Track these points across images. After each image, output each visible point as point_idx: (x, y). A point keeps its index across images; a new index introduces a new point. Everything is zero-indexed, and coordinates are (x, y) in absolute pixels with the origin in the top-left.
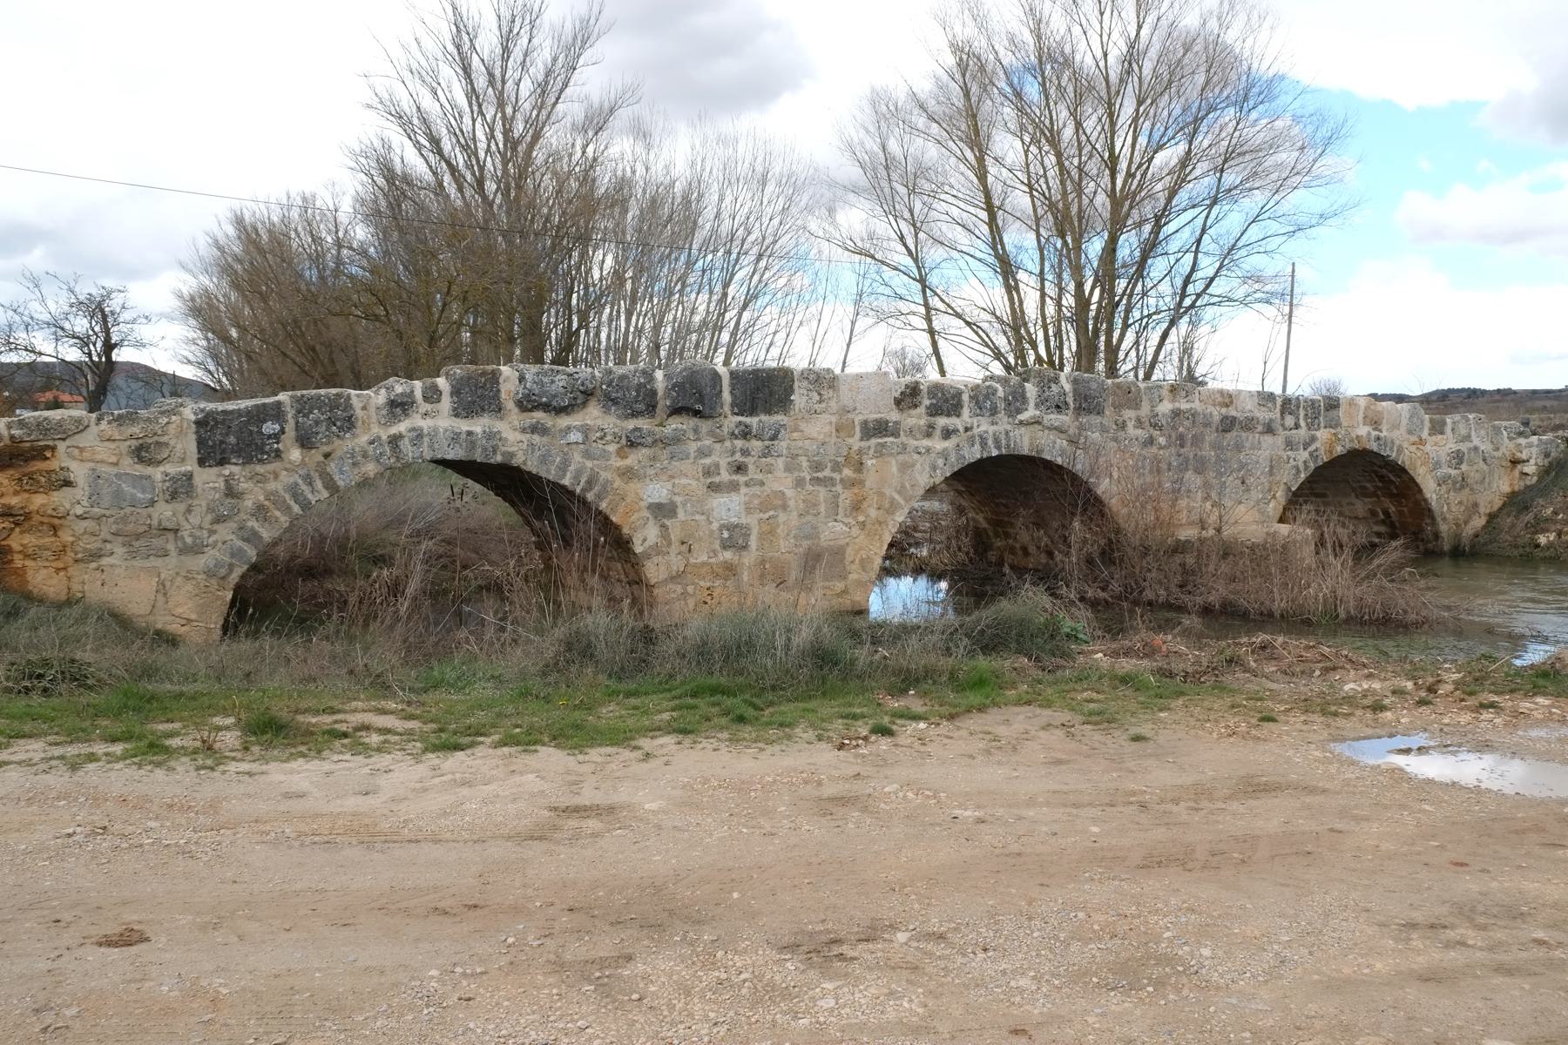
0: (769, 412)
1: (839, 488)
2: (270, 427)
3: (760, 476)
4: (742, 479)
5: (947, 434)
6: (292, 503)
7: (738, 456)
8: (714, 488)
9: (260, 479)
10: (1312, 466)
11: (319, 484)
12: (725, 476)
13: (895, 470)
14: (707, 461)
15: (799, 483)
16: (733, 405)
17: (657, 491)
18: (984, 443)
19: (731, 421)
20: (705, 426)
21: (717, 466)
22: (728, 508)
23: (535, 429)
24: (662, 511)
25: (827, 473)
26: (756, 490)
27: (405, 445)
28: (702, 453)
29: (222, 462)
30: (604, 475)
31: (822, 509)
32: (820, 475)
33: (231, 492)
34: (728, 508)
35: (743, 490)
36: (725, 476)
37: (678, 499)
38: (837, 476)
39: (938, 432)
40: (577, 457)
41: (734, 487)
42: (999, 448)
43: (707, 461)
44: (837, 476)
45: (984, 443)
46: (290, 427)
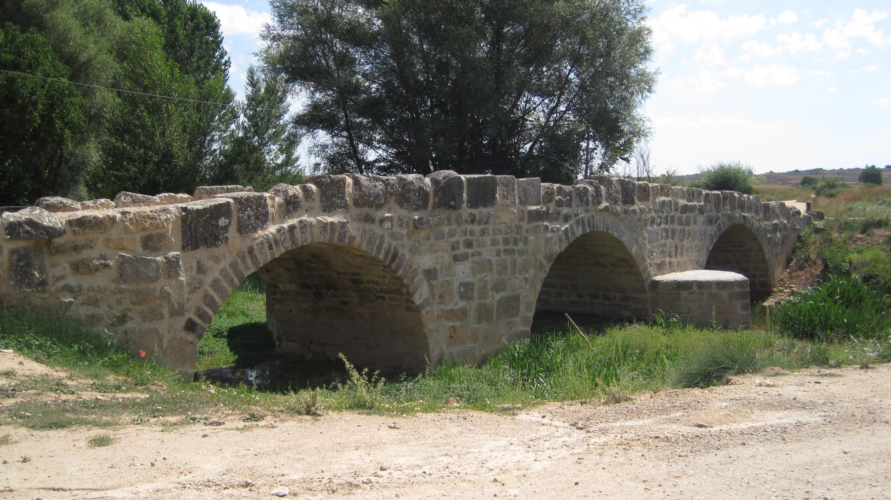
0: (485, 206)
1: (517, 256)
2: (222, 222)
3: (479, 249)
4: (470, 251)
5: (566, 219)
6: (234, 276)
7: (468, 237)
8: (456, 259)
9: (217, 260)
10: (718, 234)
11: (249, 262)
12: (462, 250)
13: (542, 243)
14: (453, 240)
15: (498, 253)
16: (469, 201)
17: (426, 261)
18: (583, 225)
19: (466, 211)
20: (454, 214)
21: (458, 242)
22: (463, 272)
23: (369, 219)
24: (430, 274)
25: (510, 246)
26: (477, 258)
27: (297, 232)
28: (452, 234)
29: (196, 247)
30: (401, 251)
31: (509, 270)
32: (507, 247)
33: (201, 270)
34: (463, 272)
35: (470, 259)
36: (462, 250)
37: (439, 267)
38: (515, 248)
39: (561, 217)
40: (387, 239)
41: (465, 257)
42: (590, 227)
43: (453, 240)
44: (515, 248)
45: (583, 225)
46: (234, 220)
